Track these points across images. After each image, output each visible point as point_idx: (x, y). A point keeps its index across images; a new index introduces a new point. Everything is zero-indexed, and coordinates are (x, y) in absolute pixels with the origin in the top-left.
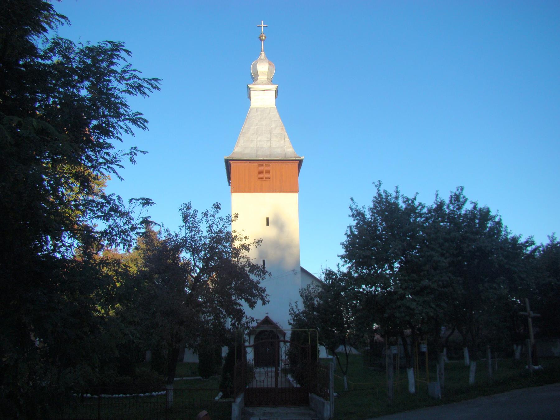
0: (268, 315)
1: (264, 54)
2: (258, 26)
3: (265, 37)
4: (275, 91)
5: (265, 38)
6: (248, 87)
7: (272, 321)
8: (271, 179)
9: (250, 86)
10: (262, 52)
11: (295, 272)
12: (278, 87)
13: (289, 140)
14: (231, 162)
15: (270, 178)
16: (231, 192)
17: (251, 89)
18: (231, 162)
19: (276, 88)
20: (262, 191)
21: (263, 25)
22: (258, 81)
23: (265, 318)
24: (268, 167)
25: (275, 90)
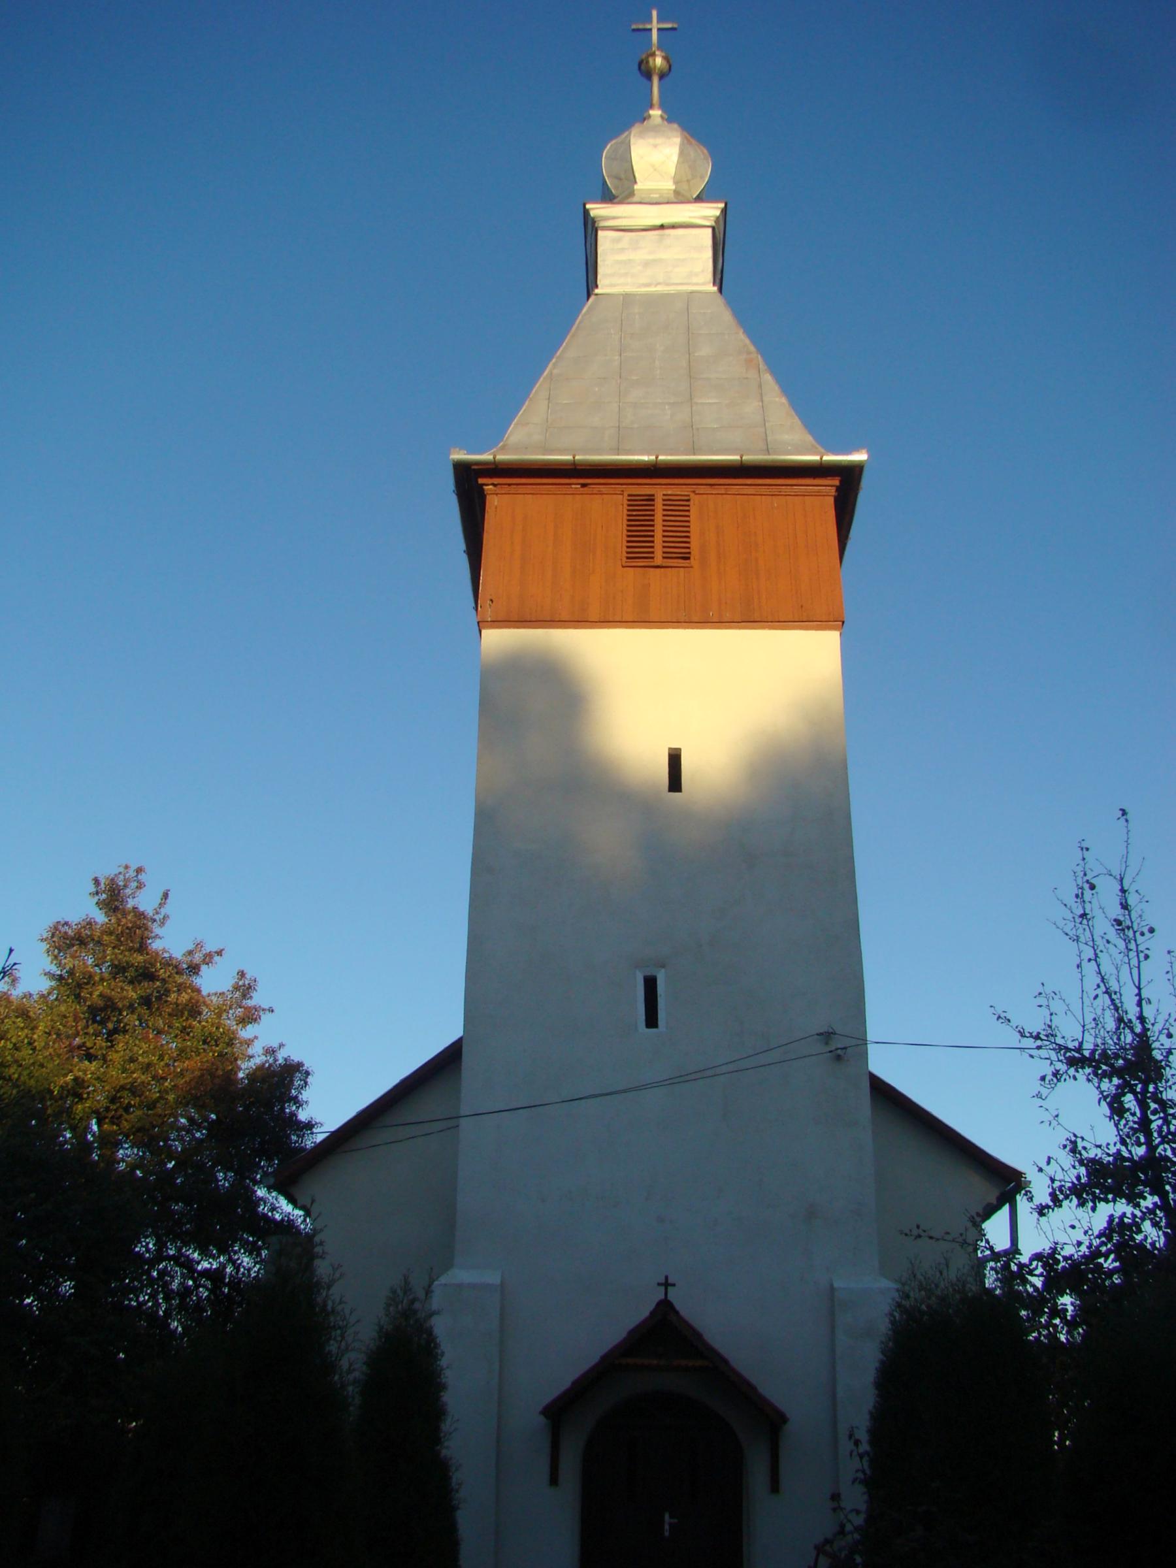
0: (670, 1297)
1: (662, 117)
2: (634, 27)
3: (666, 58)
4: (713, 228)
5: (665, 64)
6: (586, 213)
7: (699, 1336)
8: (694, 561)
9: (597, 210)
10: (651, 107)
11: (837, 1043)
12: (724, 211)
13: (784, 400)
14: (488, 485)
15: (688, 558)
16: (481, 625)
17: (602, 224)
18: (488, 485)
19: (717, 220)
20: (642, 620)
21: (658, 22)
22: (635, 199)
23: (652, 1313)
24: (678, 510)
25: (713, 223)
